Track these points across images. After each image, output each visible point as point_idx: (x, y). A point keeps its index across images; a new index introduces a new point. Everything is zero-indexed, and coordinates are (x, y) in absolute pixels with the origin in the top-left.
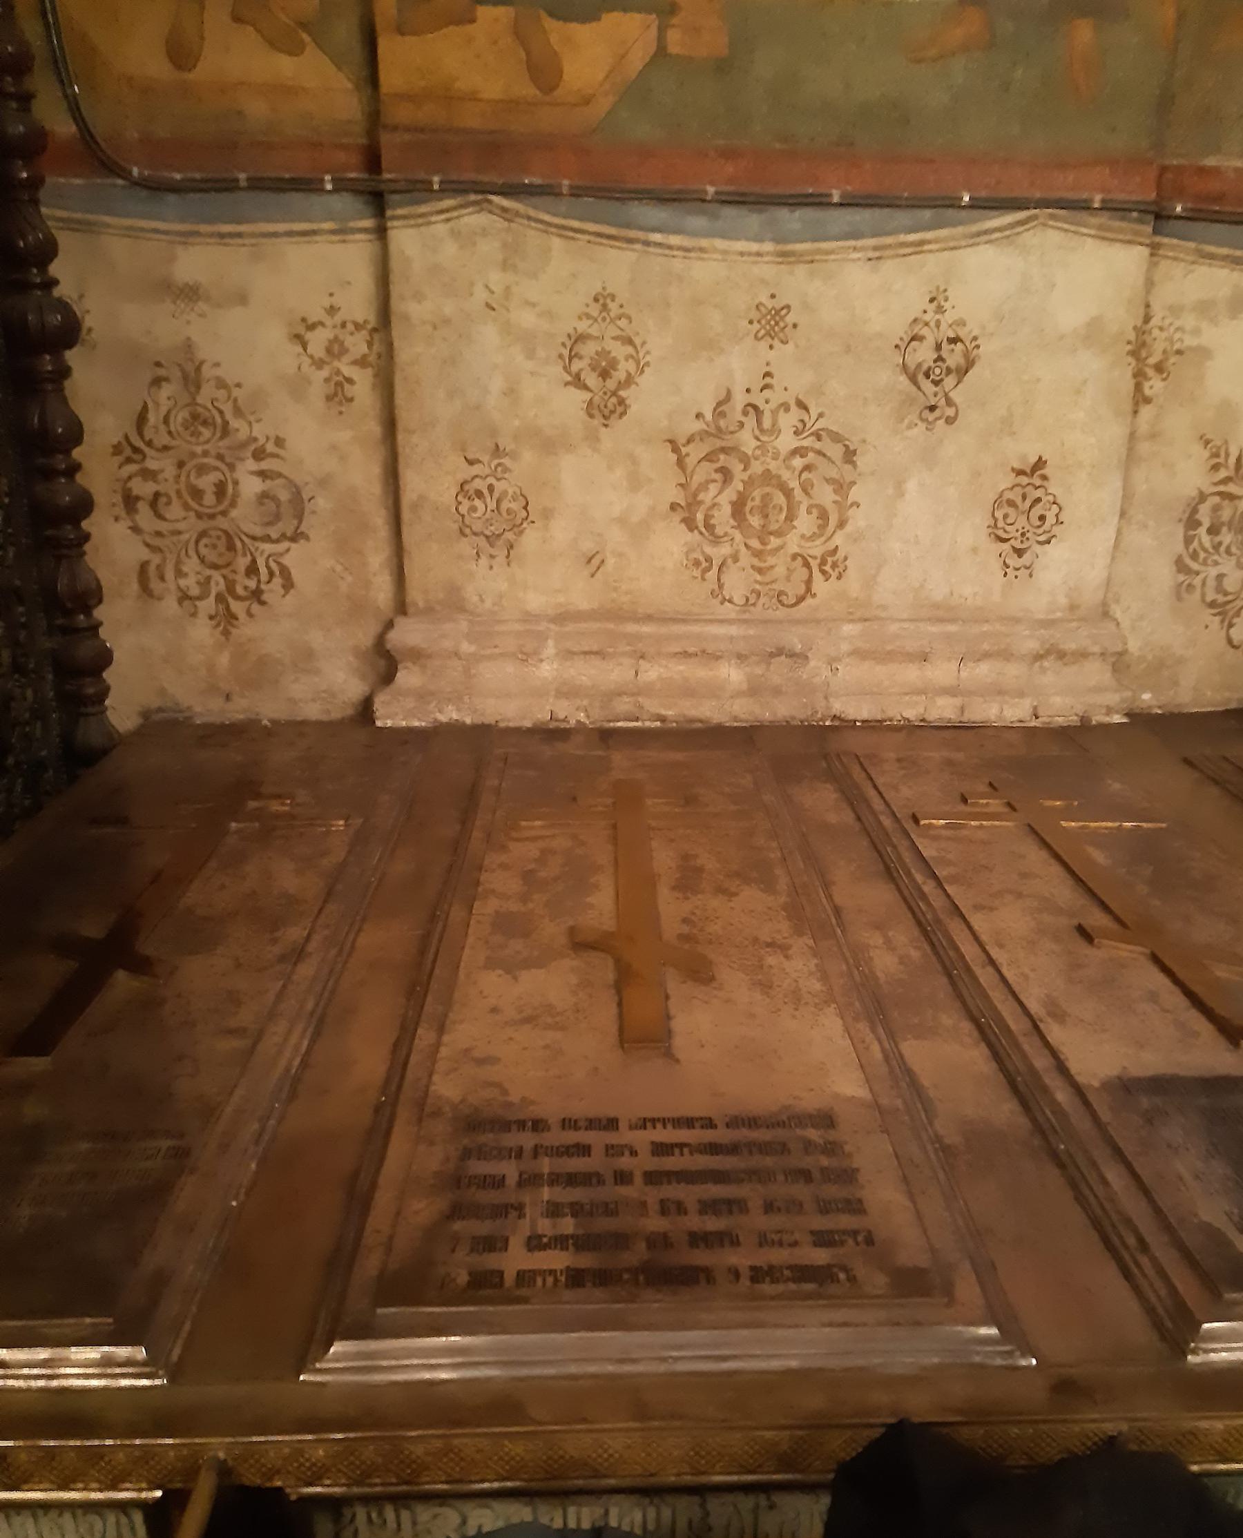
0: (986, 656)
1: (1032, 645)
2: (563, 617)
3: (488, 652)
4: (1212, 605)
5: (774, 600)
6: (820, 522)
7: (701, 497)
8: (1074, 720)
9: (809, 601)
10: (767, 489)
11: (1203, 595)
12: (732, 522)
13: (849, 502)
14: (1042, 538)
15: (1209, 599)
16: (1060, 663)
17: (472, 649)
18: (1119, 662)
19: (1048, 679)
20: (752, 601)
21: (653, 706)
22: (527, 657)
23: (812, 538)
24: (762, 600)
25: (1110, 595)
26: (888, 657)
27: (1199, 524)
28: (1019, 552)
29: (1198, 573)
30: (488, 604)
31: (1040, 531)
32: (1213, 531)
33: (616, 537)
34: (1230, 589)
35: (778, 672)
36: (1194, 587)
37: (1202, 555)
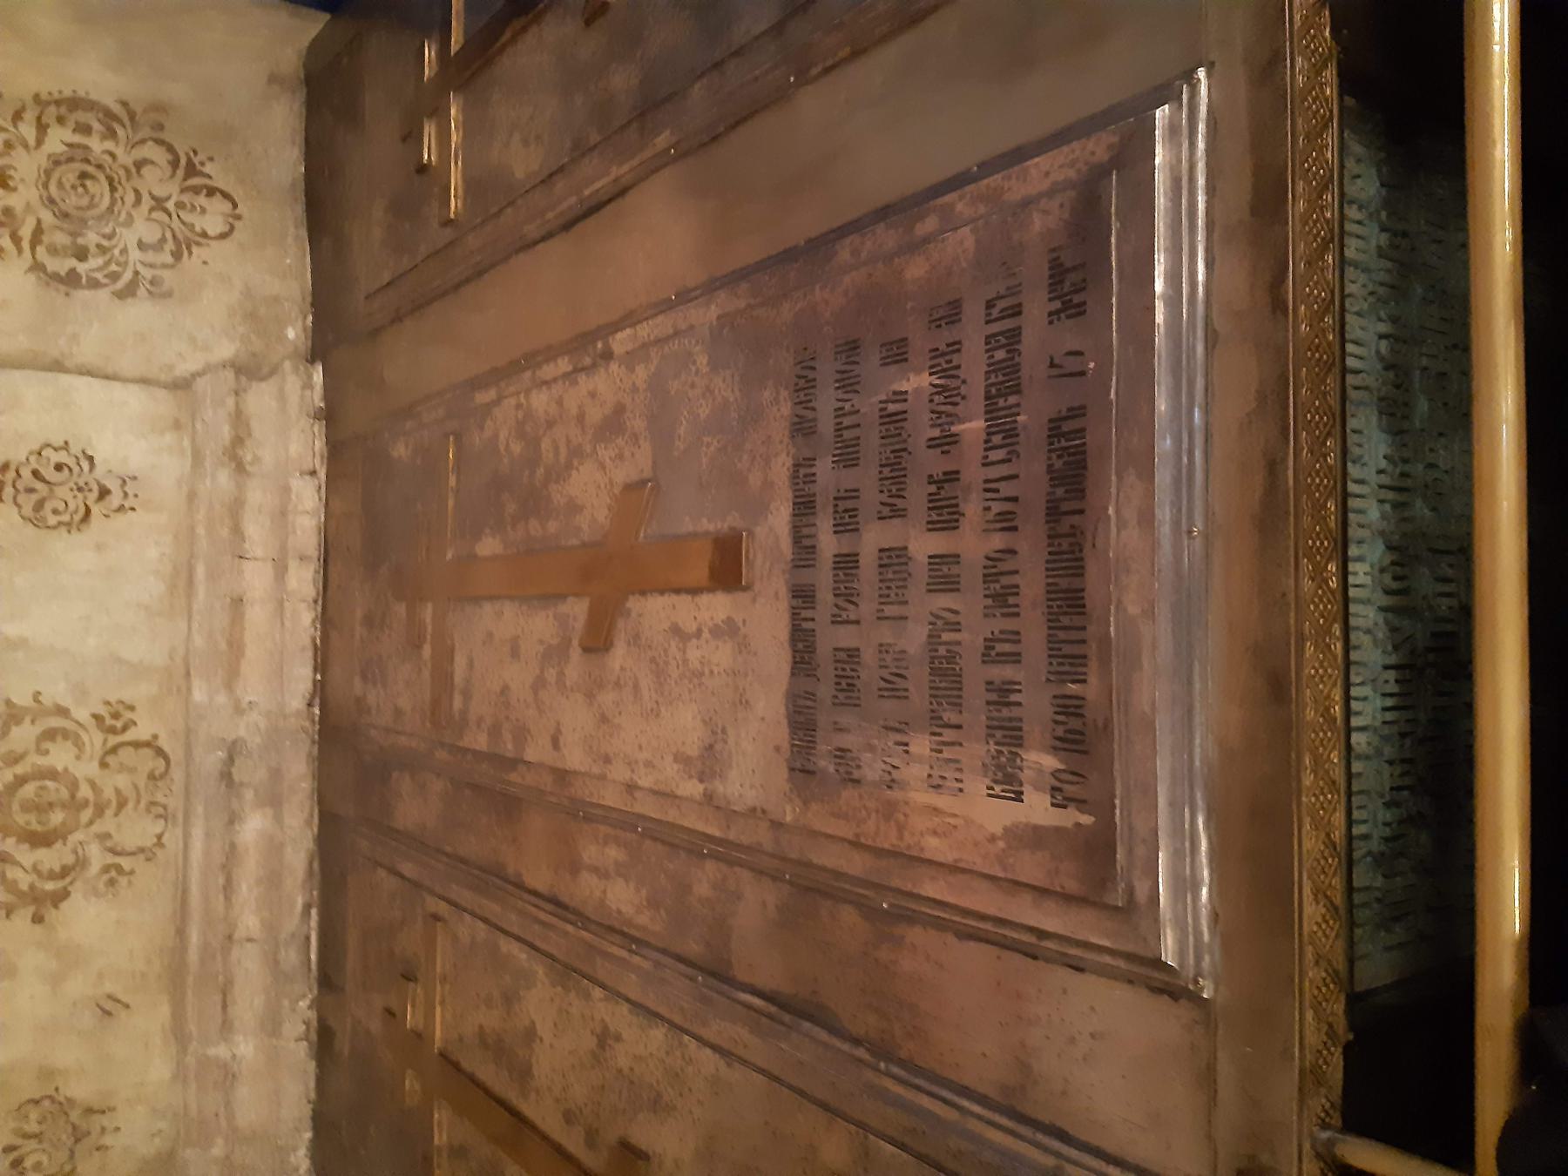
0: (237, 531)
1: (224, 478)
2: (178, 1034)
3: (224, 1123)
4: (177, 255)
5: (160, 784)
6: (59, 738)
7: (24, 887)
8: (319, 428)
9: (163, 743)
10: (16, 807)
11: (165, 266)
12: (58, 845)
13: (34, 705)
14: (85, 465)
15: (169, 259)
16: (248, 442)
17: (220, 1141)
18: (248, 370)
19: (268, 456)
20: (161, 810)
21: (292, 923)
22: (228, 1075)
23: (79, 744)
24: (160, 798)
25: (163, 377)
26: (236, 648)
27: (73, 271)
28: (104, 493)
29: (137, 273)
30: (162, 1125)
31: (76, 469)
32: (82, 255)
33: (78, 986)
34: (159, 236)
35: (250, 772)
36: (154, 277)
37: (114, 267)
